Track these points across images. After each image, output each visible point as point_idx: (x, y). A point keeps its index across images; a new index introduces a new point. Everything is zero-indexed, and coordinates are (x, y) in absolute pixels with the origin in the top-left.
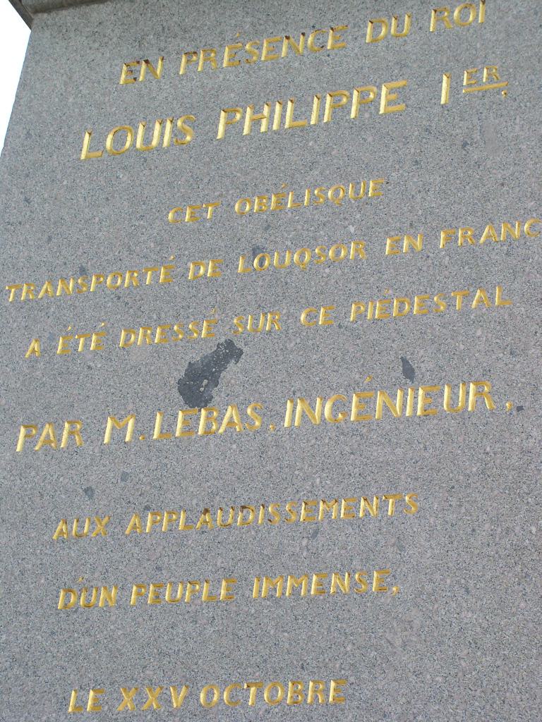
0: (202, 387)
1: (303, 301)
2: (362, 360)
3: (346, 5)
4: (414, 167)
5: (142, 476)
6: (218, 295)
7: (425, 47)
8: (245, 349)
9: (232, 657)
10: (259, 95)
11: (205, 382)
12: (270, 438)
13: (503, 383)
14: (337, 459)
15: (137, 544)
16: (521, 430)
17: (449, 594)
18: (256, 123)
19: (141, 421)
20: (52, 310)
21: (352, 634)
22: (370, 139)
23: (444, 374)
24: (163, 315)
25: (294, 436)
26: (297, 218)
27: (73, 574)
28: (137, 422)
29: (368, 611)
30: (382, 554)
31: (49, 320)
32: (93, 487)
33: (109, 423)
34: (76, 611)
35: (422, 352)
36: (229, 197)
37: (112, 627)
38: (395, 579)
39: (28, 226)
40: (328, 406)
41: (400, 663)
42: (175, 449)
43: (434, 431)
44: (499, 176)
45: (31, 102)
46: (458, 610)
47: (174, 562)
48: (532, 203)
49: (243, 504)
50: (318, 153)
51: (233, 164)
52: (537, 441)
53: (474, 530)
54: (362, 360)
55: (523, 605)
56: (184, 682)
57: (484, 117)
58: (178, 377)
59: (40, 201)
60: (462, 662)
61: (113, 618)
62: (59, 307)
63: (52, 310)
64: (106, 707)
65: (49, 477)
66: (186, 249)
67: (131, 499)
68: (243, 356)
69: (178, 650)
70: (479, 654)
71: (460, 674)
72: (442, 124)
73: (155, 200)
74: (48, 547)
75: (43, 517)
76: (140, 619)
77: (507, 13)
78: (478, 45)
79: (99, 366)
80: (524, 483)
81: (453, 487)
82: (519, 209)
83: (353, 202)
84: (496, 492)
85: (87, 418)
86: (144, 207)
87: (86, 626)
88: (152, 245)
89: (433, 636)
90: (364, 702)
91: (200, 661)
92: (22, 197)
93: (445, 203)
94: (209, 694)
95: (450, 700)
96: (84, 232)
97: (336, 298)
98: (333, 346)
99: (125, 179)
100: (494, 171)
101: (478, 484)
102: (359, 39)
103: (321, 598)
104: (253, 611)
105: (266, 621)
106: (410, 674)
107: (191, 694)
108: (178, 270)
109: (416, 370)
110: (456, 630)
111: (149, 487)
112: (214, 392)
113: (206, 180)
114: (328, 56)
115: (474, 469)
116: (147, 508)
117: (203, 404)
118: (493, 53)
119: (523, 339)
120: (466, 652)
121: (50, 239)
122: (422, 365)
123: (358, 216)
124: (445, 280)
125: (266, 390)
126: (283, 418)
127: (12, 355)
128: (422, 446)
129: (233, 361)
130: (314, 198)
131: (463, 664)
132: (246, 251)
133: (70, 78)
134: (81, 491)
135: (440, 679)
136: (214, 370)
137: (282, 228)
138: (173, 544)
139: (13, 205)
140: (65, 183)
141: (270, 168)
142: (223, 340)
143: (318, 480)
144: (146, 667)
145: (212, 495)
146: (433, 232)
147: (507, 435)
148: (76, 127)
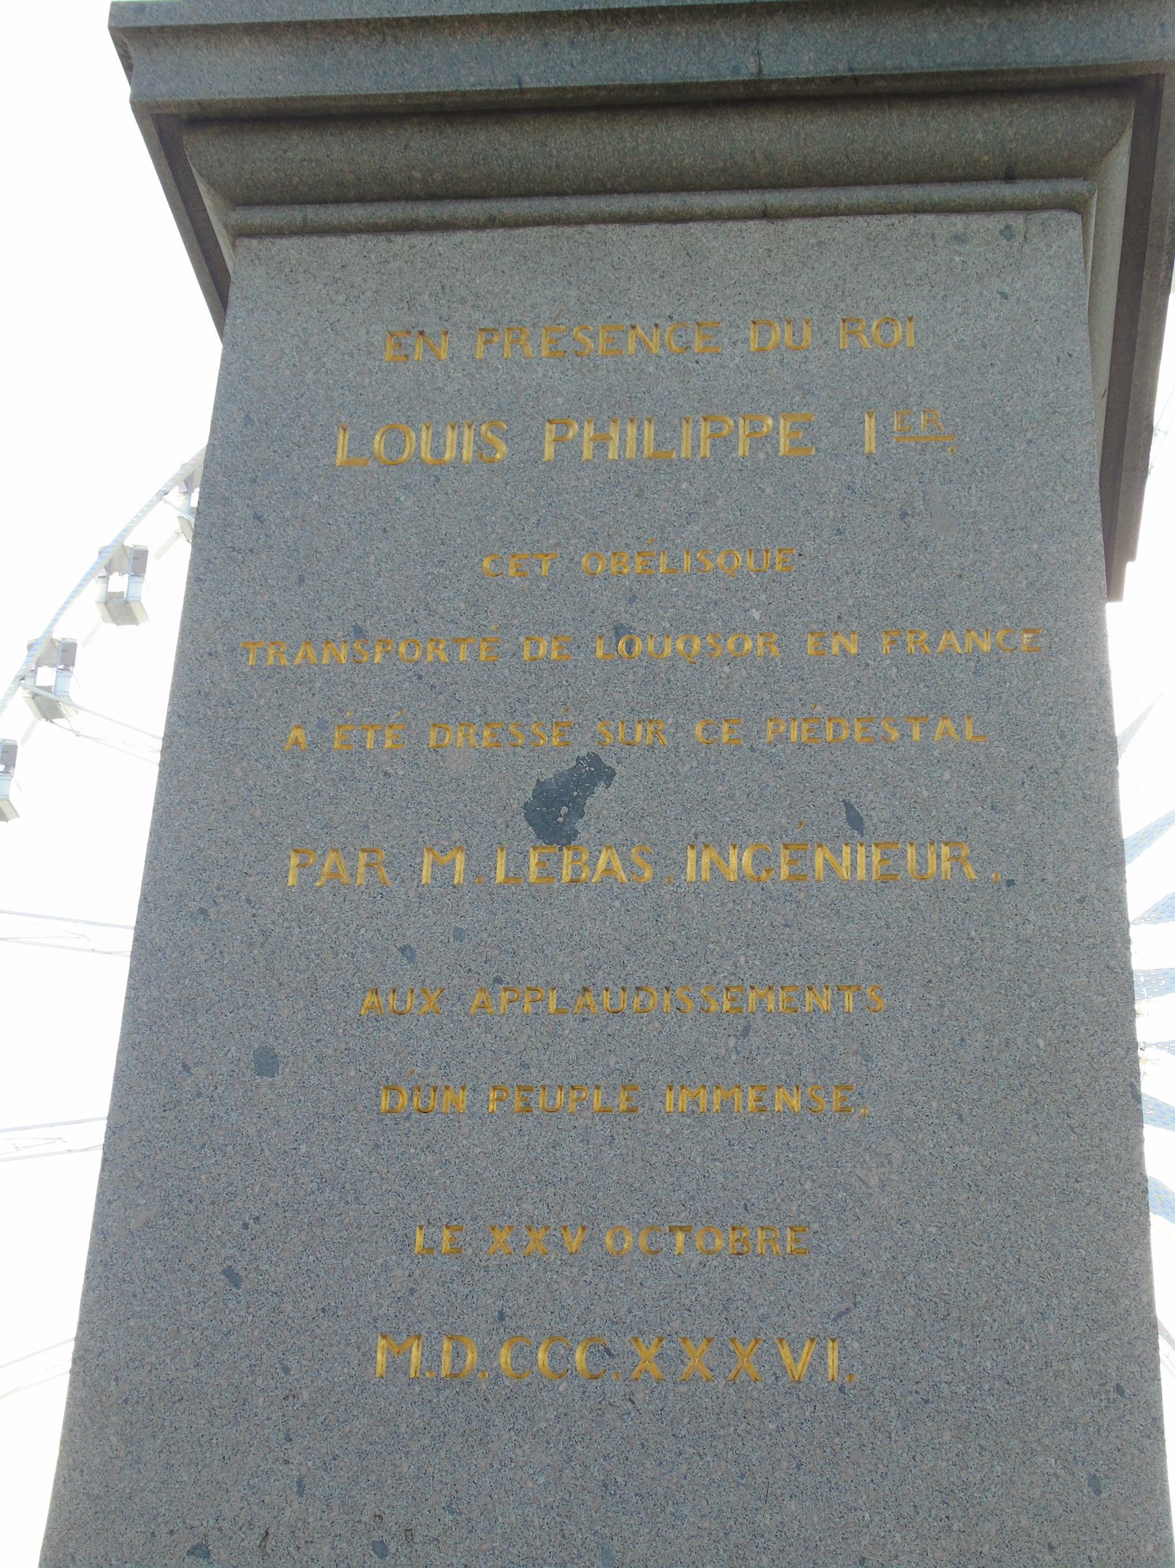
0: (561, 816)
1: (696, 708)
2: (789, 799)
3: (715, 293)
4: (836, 538)
5: (485, 935)
6: (569, 688)
7: (835, 369)
8: (618, 769)
9: (645, 1191)
10: (601, 406)
11: (564, 810)
12: (668, 896)
13: (985, 846)
15: (488, 1030)
16: (1015, 911)
17: (937, 1121)
18: (601, 444)
19: (474, 857)
21: (810, 1167)
22: (769, 490)
23: (904, 828)
24: (490, 709)
25: (702, 895)
27: (397, 1065)
28: (469, 858)
29: (829, 1138)
32: (414, 946)
33: (427, 859)
34: (408, 1118)
35: (871, 796)
36: (571, 548)
37: (465, 1142)
38: (863, 1098)
39: (264, 557)
40: (747, 857)
41: (879, 1208)
43: (898, 904)
44: (955, 564)
46: (951, 1143)
47: (546, 1057)
48: (1003, 607)
49: (638, 985)
50: (696, 500)
51: (572, 502)
52: (1037, 928)
53: (963, 1040)
54: (789, 799)
55: (1034, 1139)
57: (927, 480)
58: (523, 800)
59: (278, 520)
60: (961, 1209)
61: (466, 1130)
62: (328, 681)
64: (470, 1251)
65: (342, 926)
67: (473, 967)
68: (616, 778)
69: (567, 1179)
70: (982, 1199)
71: (959, 1224)
72: (870, 482)
73: (459, 540)
74: (355, 1025)
75: (342, 983)
76: (506, 1134)
77: (944, 339)
78: (910, 380)
79: (401, 773)
80: (1025, 982)
81: (930, 981)
83: (754, 576)
84: (988, 992)
85: (392, 847)
87: (426, 1138)
88: (463, 606)
89: (920, 1175)
90: (835, 1256)
91: (600, 1195)
93: (883, 592)
94: (619, 1238)
95: (949, 1257)
96: (354, 575)
97: (743, 709)
98: (745, 776)
99: (409, 503)
100: (948, 557)
101: (964, 979)
102: (739, 344)
103: (763, 1118)
104: (668, 1131)
105: (688, 1145)
106: (893, 1223)
107: (591, 1238)
108: (506, 646)
109: (865, 819)
110: (950, 1168)
111: (497, 952)
112: (579, 825)
113: (533, 520)
114: (697, 362)
115: (957, 959)
116: (498, 981)
117: (564, 841)
118: (931, 392)
119: (1007, 791)
120: (964, 1196)
121: (301, 579)
122: (873, 813)
123: (763, 597)
124: (894, 699)
125: (655, 828)
126: (683, 869)
127: (262, 745)
128: (883, 923)
129: (603, 784)
131: (963, 1211)
132: (604, 630)
133: (306, 343)
134: (395, 950)
135: (934, 1230)
136: (575, 794)
137: (654, 602)
138: (542, 1034)
139: (237, 523)
140: (315, 498)
141: (627, 514)
142: (584, 753)
143: (742, 959)
144: (521, 1198)
146: (872, 632)
147: (997, 917)
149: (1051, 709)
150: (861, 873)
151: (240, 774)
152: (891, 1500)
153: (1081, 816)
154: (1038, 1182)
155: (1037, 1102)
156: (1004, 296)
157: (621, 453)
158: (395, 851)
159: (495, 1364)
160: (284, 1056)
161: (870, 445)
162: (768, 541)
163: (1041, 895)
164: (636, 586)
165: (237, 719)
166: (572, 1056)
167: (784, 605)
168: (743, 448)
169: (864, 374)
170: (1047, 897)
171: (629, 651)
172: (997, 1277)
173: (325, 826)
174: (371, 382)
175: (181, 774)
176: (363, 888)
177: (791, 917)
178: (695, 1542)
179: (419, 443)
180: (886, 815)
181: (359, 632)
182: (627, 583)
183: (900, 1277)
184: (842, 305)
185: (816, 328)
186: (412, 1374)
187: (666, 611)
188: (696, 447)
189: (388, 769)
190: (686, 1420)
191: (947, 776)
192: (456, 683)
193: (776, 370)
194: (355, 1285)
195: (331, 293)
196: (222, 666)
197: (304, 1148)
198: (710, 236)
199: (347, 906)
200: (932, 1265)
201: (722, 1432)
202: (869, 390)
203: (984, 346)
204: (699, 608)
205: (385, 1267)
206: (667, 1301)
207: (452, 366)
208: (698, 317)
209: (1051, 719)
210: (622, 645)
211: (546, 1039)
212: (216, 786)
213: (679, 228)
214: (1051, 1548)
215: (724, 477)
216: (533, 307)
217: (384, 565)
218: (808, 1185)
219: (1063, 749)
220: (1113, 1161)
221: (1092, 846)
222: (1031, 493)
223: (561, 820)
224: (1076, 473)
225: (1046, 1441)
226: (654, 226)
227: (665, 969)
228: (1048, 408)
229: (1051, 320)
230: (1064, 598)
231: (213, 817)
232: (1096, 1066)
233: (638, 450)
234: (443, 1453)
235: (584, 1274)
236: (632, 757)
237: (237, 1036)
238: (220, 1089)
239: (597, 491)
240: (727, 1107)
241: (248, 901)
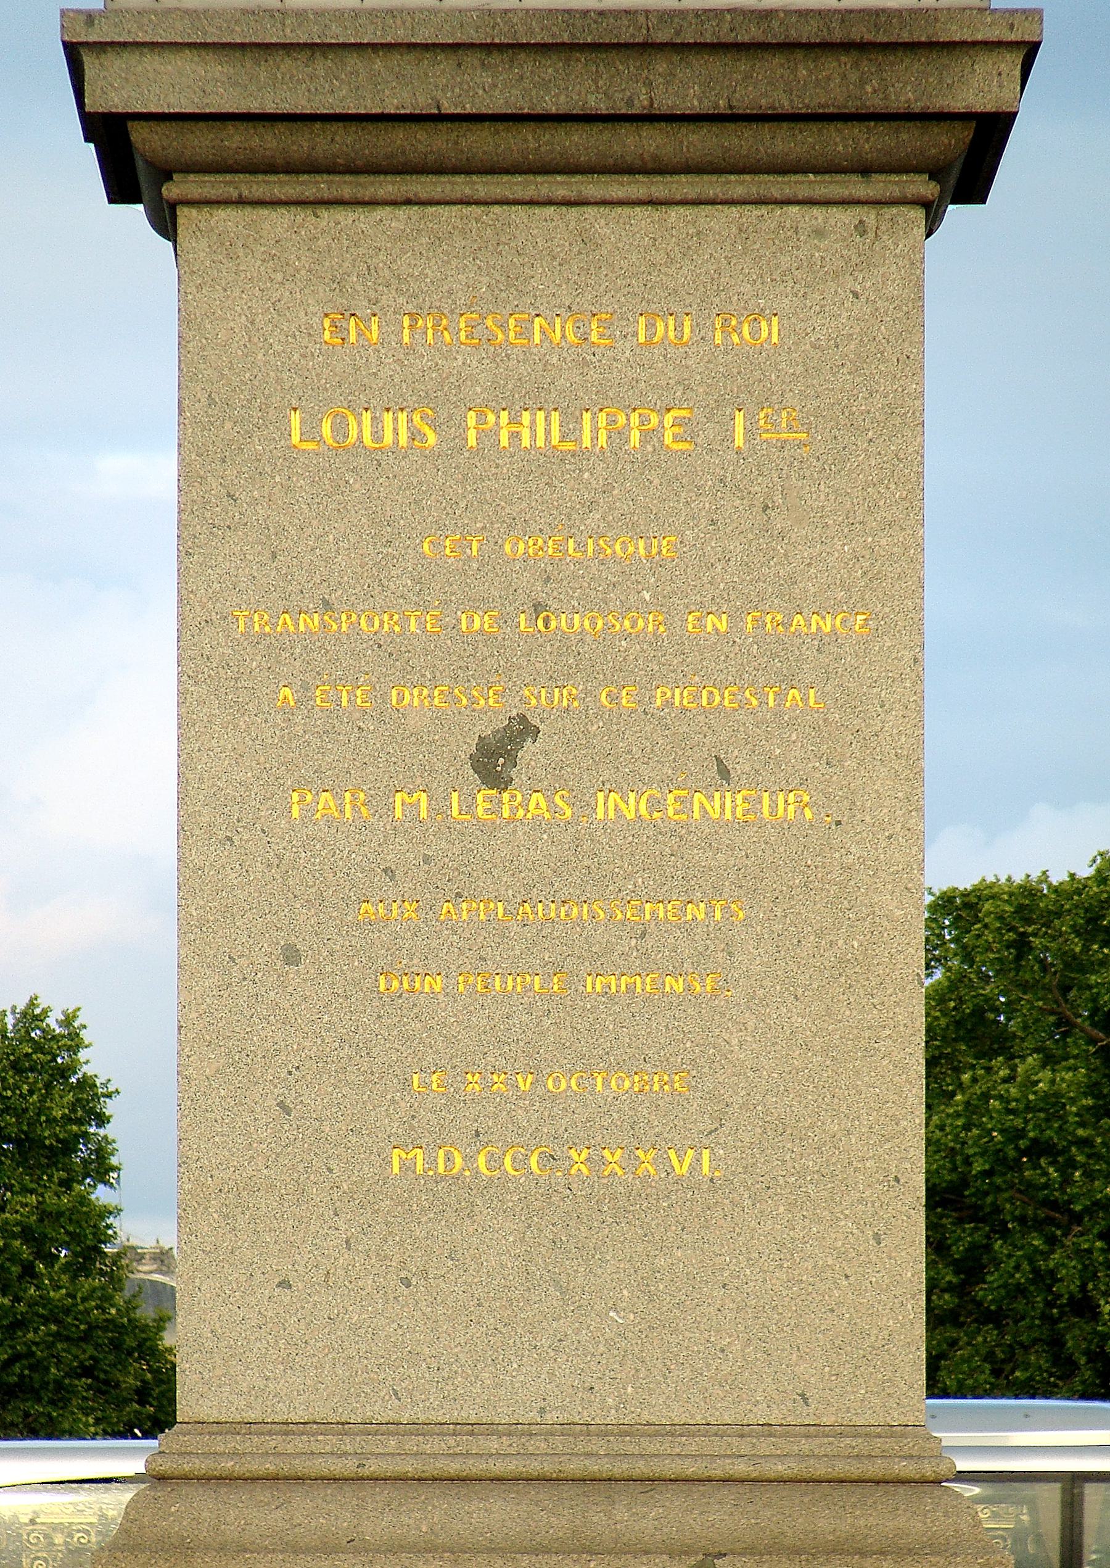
2: (674, 754)
4: (710, 528)
5: (446, 860)
7: (711, 366)
11: (501, 760)
14: (658, 859)
20: (298, 651)
22: (656, 482)
24: (438, 674)
26: (581, 572)
28: (430, 799)
29: (704, 1011)
30: (712, 959)
31: (297, 663)
34: (400, 996)
35: (736, 752)
37: (443, 1014)
42: (479, 833)
43: (755, 839)
44: (806, 554)
45: (203, 349)
46: (789, 1015)
47: (498, 953)
53: (799, 941)
55: (848, 1013)
56: (528, 1070)
60: (795, 1061)
63: (298, 651)
64: (452, 1090)
65: (338, 852)
66: (452, 594)
68: (540, 735)
70: (810, 1054)
71: (794, 1072)
79: (372, 728)
80: (845, 899)
82: (828, 598)
84: (819, 906)
86: (389, 529)
92: (224, 491)
97: (638, 678)
99: (357, 486)
101: (801, 896)
104: (589, 1007)
111: (456, 873)
112: (513, 773)
113: (463, 504)
115: (797, 881)
116: (459, 895)
119: (839, 750)
120: (798, 1052)
121: (274, 556)
126: (595, 811)
129: (530, 739)
130: (599, 550)
131: (796, 1063)
133: (252, 323)
135: (776, 1075)
136: (509, 747)
137: (565, 583)
140: (278, 479)
142: (514, 713)
145: (529, 888)
148: (275, 400)
149: (875, 682)
150: (728, 815)
151: (244, 727)
152: (744, 1249)
153: (893, 771)
154: (849, 1043)
155: (851, 986)
156: (856, 295)
157: (533, 443)
158: (372, 792)
159: (475, 1166)
160: (304, 951)
161: (739, 441)
162: (655, 529)
163: (859, 833)
164: (549, 568)
165: (236, 679)
166: (518, 952)
167: (669, 588)
168: (635, 437)
169: (735, 371)
170: (865, 834)
171: (547, 627)
172: (818, 1107)
173: (316, 772)
174: (313, 365)
175: (197, 725)
176: (350, 821)
177: (676, 848)
178: (615, 1276)
179: (361, 428)
180: (747, 768)
181: (327, 605)
182: (543, 565)
183: (752, 1107)
184: (717, 300)
185: (695, 323)
186: (418, 1173)
187: (574, 590)
188: (595, 438)
189: (361, 724)
190: (607, 1201)
191: (794, 737)
192: (409, 652)
193: (660, 365)
194: (372, 1113)
195: (269, 271)
196: (218, 633)
197: (326, 1018)
198: (603, 222)
199: (339, 835)
200: (774, 1099)
201: (632, 1208)
202: (739, 387)
203: (837, 347)
204: (600, 589)
205: (393, 1101)
206: (592, 1123)
207: (383, 351)
208: (593, 308)
209: (875, 690)
210: (540, 622)
211: (497, 940)
212: (226, 737)
213: (574, 211)
214: (847, 1277)
215: (619, 469)
216: (450, 292)
217: (341, 544)
218: (688, 1045)
219: (883, 715)
220: (902, 1028)
221: (900, 794)
222: (869, 490)
223: (499, 769)
224: (907, 471)
225: (847, 1212)
226: (552, 208)
227: (583, 888)
228: (887, 408)
229: (894, 321)
230: (890, 586)
231: (227, 762)
232: (894, 961)
233: (546, 440)
234: (443, 1223)
235: (533, 1105)
236: (552, 717)
237: (267, 935)
238: (260, 975)
239: (513, 479)
240: (631, 989)
241: (263, 831)
